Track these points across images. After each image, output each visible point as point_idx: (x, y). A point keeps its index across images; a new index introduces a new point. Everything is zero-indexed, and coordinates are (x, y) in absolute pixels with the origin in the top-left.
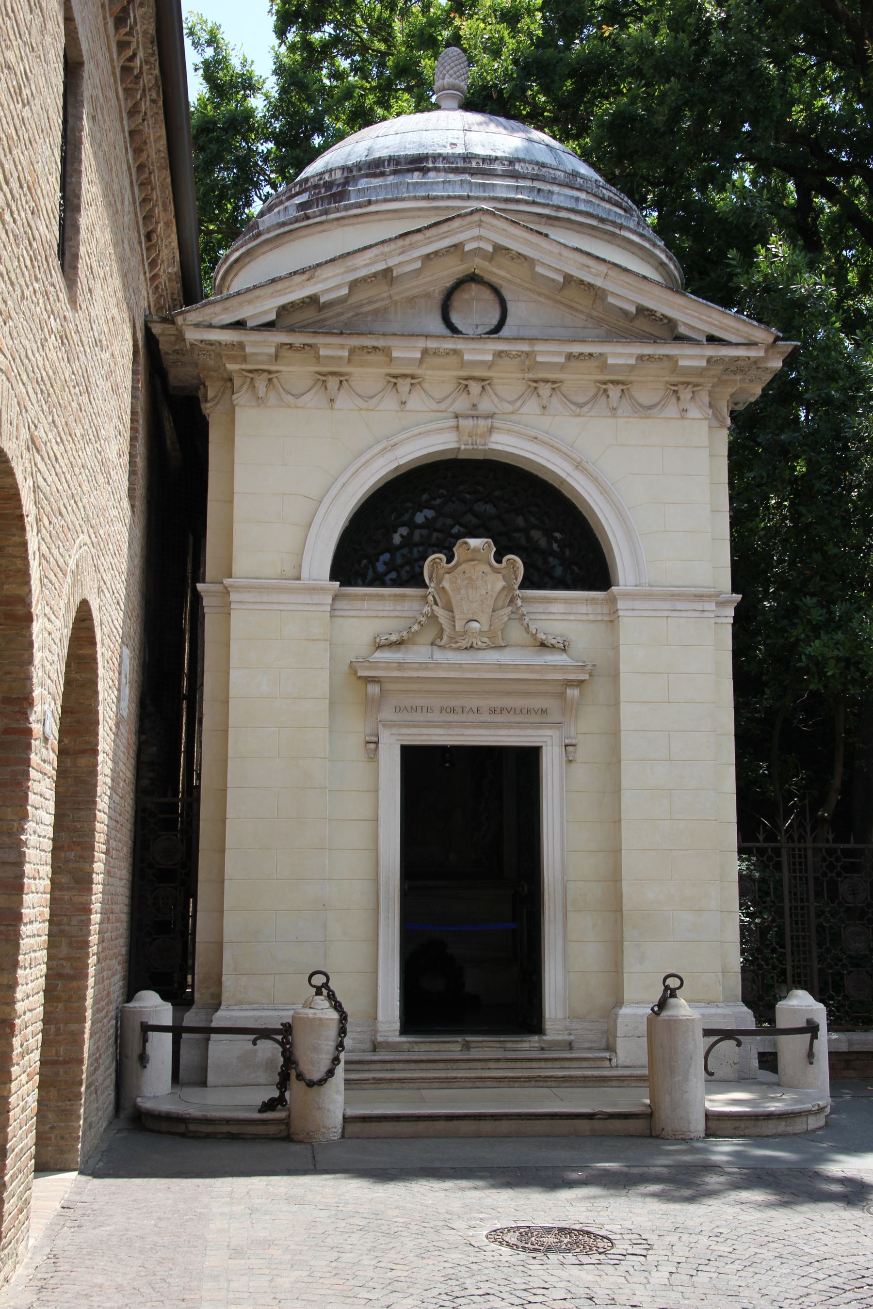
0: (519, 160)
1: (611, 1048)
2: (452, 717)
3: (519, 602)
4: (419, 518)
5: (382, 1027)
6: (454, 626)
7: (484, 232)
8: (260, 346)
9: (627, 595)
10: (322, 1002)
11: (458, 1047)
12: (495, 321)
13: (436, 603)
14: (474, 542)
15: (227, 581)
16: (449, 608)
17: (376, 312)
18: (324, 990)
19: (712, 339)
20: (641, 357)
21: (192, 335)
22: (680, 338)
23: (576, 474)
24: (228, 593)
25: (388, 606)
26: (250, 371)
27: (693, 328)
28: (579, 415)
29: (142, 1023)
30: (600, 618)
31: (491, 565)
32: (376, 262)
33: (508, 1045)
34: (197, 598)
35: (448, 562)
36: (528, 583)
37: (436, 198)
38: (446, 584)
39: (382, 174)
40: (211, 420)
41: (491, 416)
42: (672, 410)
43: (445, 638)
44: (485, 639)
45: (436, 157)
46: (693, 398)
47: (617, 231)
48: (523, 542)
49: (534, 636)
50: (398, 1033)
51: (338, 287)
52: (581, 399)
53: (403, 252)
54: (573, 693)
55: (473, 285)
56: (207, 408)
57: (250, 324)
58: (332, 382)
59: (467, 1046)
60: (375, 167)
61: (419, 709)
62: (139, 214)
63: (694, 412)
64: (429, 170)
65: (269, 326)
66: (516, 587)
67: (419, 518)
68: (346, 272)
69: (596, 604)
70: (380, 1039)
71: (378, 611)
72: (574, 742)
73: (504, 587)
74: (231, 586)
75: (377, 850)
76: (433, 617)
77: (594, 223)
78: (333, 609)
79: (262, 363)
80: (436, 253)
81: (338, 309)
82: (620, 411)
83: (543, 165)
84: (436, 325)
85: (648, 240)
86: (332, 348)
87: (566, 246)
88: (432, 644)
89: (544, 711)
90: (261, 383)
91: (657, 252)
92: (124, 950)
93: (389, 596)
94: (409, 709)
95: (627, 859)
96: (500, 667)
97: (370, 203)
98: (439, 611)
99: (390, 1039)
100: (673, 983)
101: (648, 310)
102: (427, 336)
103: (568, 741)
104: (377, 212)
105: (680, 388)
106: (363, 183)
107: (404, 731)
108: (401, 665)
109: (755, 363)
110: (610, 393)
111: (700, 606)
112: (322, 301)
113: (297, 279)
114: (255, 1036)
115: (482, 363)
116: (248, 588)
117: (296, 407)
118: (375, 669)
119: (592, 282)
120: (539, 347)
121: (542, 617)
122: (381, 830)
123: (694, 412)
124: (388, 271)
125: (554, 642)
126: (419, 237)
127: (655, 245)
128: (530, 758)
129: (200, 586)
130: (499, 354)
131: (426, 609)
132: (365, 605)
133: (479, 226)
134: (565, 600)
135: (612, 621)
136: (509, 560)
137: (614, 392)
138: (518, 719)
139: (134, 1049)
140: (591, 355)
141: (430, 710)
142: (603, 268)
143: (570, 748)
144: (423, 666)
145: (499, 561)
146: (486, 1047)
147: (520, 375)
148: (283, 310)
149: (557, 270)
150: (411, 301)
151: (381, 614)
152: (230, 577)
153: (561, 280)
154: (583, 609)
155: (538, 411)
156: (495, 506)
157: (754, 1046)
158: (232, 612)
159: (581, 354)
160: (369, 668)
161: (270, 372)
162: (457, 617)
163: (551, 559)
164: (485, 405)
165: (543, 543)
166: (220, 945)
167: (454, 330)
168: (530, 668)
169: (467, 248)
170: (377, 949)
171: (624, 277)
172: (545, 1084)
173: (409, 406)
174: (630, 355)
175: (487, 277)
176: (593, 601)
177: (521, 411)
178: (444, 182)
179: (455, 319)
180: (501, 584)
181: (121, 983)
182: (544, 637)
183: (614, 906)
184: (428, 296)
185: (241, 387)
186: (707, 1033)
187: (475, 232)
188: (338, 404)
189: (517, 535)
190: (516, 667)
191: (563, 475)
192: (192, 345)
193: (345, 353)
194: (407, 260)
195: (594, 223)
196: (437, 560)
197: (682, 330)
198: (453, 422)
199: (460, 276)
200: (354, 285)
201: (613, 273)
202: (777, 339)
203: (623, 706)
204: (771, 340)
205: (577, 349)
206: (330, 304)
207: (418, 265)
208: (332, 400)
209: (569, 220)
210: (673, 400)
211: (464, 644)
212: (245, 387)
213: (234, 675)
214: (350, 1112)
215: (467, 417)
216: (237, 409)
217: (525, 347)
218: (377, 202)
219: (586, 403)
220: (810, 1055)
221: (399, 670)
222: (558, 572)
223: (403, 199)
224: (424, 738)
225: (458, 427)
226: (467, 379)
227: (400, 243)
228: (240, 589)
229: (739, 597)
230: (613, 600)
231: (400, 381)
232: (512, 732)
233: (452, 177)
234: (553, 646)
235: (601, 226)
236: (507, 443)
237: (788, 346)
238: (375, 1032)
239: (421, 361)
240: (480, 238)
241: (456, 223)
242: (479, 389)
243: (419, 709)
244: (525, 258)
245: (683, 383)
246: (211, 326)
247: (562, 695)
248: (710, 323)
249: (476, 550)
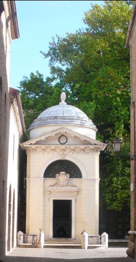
8: (34, 147)
21: (25, 146)
34: (25, 180)
54: (76, 193)
84: (57, 142)
86: (44, 147)
90: (34, 151)
148: (37, 142)
220: (105, 240)
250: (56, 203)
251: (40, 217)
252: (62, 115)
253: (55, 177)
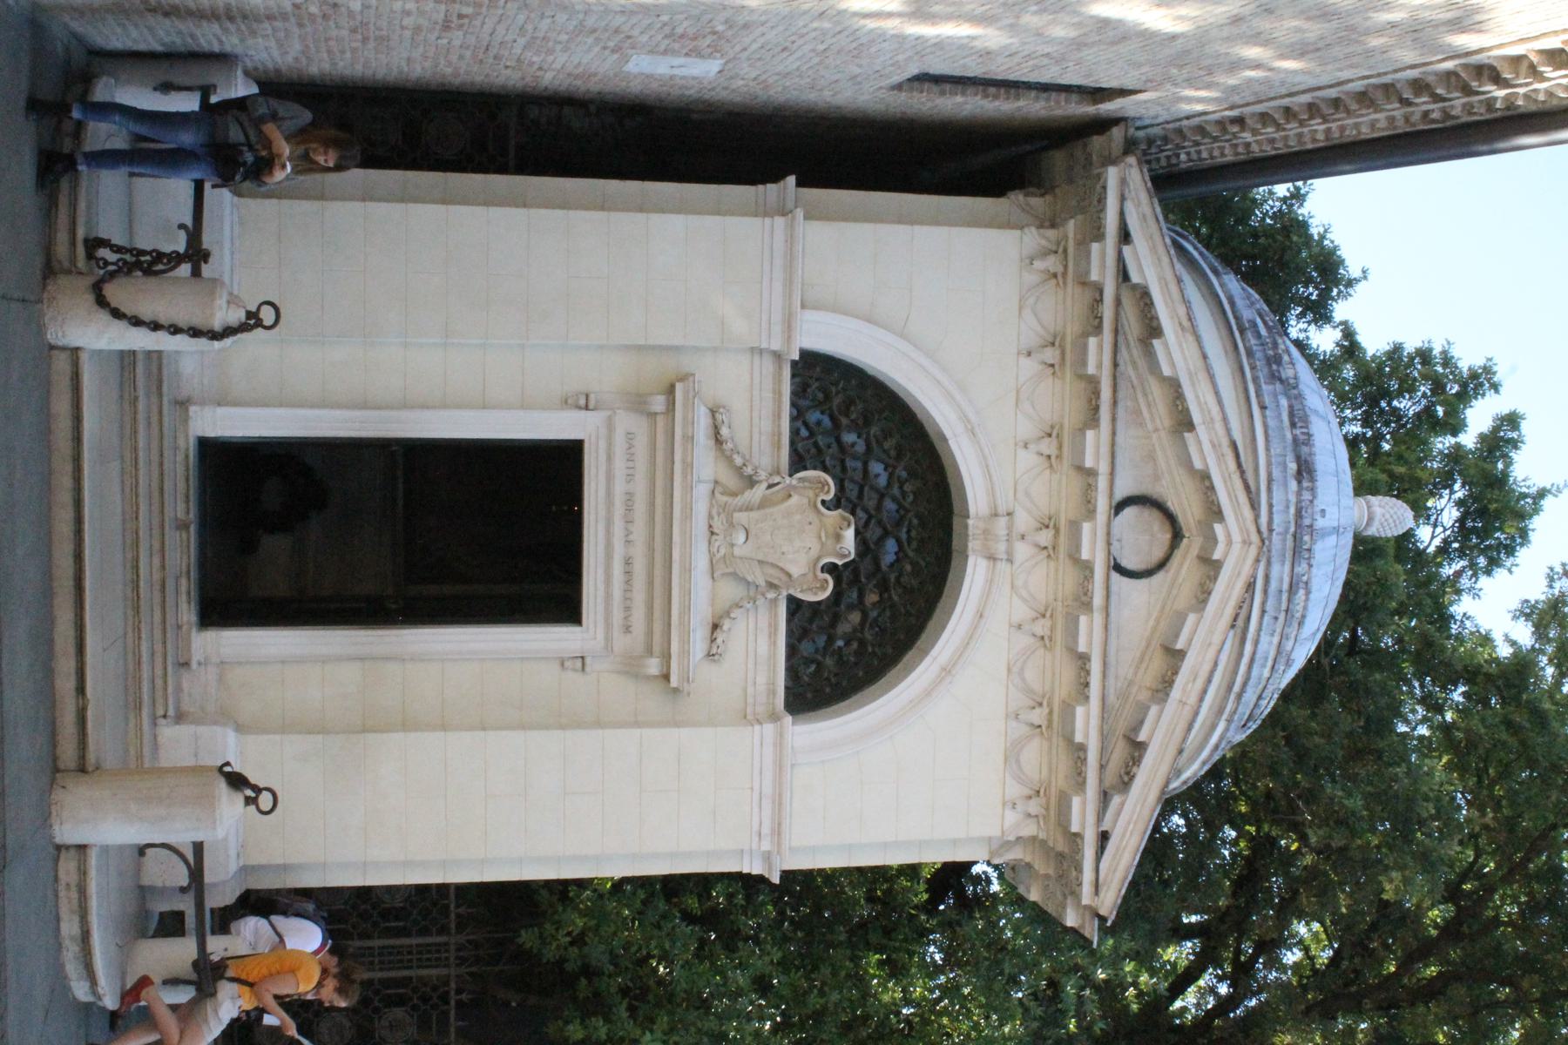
0: (1308, 593)
1: (180, 718)
2: (619, 510)
3: (771, 595)
4: (876, 468)
5: (208, 412)
7: (1237, 547)
9: (781, 735)
10: (236, 316)
11: (181, 515)
12: (1125, 563)
13: (770, 486)
14: (849, 535)
15: (800, 213)
16: (764, 504)
17: (1138, 412)
18: (252, 321)
19: (1104, 837)
20: (1082, 748)
21: (1112, 174)
22: (1105, 797)
23: (935, 668)
24: (784, 215)
25: (766, 425)
26: (1065, 251)
27: (1118, 814)
28: (1009, 670)
29: (215, 87)
30: (750, 700)
31: (818, 559)
32: (1202, 410)
33: (184, 581)
35: (823, 502)
36: (795, 606)
37: (1269, 489)
38: (795, 499)
39: (1293, 425)
40: (1001, 200)
41: (1010, 561)
42: (1015, 790)
43: (725, 498)
44: (723, 551)
45: (1312, 490)
46: (1029, 815)
47: (1225, 716)
48: (845, 601)
49: (727, 614)
50: (201, 434)
51: (1173, 365)
52: (1030, 675)
53: (1214, 446)
54: (653, 666)
55: (1168, 536)
56: (1017, 197)
57: (1126, 250)
58: (1051, 355)
59: (183, 526)
60: (1298, 418)
61: (631, 464)
62: (1272, 104)
63: (1011, 817)
64: (1299, 482)
65: (1123, 275)
66: (792, 592)
67: (876, 468)
68: (1190, 374)
70: (192, 409)
71: (760, 412)
72: (588, 669)
73: (790, 576)
74: (794, 218)
75: (444, 406)
76: (751, 482)
77: (1236, 688)
78: (761, 351)
79: (1076, 265)
80: (1212, 488)
81: (1142, 363)
82: (1014, 724)
83: (1301, 624)
85: (1211, 755)
86: (1097, 354)
87: (1220, 651)
88: (716, 482)
89: (627, 629)
91: (1196, 766)
92: (314, 70)
95: (433, 739)
96: (687, 570)
97: (1263, 408)
98: (759, 491)
99: (191, 424)
100: (265, 800)
101: (1141, 757)
102: (1112, 473)
103: (588, 661)
104: (1251, 416)
105: (1043, 800)
106: (1284, 402)
107: (603, 444)
108: (689, 439)
109: (1073, 893)
110: (1038, 710)
111: (766, 830)
112: (1156, 342)
113: (1182, 311)
114: (189, 223)
115: (1078, 547)
116: (791, 240)
117: (1021, 309)
118: (685, 406)
119: (1176, 686)
120: (1098, 618)
121: (752, 625)
122: (472, 413)
123: (1011, 817)
124: (1190, 426)
125: (719, 641)
126: (1232, 465)
127: (1204, 763)
128: (567, 609)
129: (791, 180)
130: (1087, 567)
131: (763, 475)
132: (768, 395)
133: (1244, 542)
134: (772, 656)
135: (746, 718)
137: (1038, 716)
138: (617, 592)
139: (178, 78)
140: (1087, 685)
141: (630, 477)
142: (1193, 700)
143: (579, 663)
144: (688, 466)
146: (182, 552)
147: (1060, 595)
148: (1144, 295)
149: (1190, 641)
150: (1151, 457)
151: (755, 414)
152: (806, 218)
153: (1179, 646)
154: (762, 680)
155: (1016, 619)
156: (892, 565)
157: (186, 905)
158: (757, 221)
159: (1088, 673)
160: (686, 398)
161: (1065, 274)
163: (824, 638)
164: (1022, 551)
165: (844, 628)
166: (322, 197)
167: (1120, 507)
168: (686, 609)
169: (1218, 528)
170: (312, 406)
171: (1182, 725)
172: (130, 630)
173: (1022, 453)
174: (1087, 735)
175: (1178, 554)
176: (772, 692)
177: (1015, 599)
178: (1288, 501)
179: (1130, 512)
180: (795, 571)
181: (270, 66)
182: (725, 628)
183: (370, 724)
184: (1157, 478)
185: (1044, 237)
186: (198, 848)
187: (1237, 538)
188: (1024, 361)
189: (855, 595)
190: (687, 593)
191: (934, 652)
192: (1099, 176)
193: (1091, 370)
194: (1206, 447)
195: (1236, 688)
197: (1116, 800)
198: (1002, 509)
199: (1181, 519)
200: (1174, 386)
201: (1187, 712)
202: (1102, 919)
203: (637, 732)
204: (1102, 912)
205: (1095, 666)
206: (1150, 354)
207: (1198, 465)
208: (1029, 354)
209: (1240, 655)
210: (1027, 792)
211: (718, 525)
212: (1043, 242)
213: (677, 222)
214: (84, 357)
215: (1010, 527)
216: (1017, 232)
217: (1098, 601)
218: (1264, 417)
219: (1024, 680)
222: (806, 648)
223: (1268, 449)
225: (996, 515)
226: (1057, 530)
227: (1225, 442)
228: (791, 227)
229: (776, 880)
230: (774, 717)
231: (1054, 440)
232: (601, 587)
233: (1292, 510)
234: (713, 640)
235: (1232, 697)
236: (975, 578)
237: (1092, 932)
238: (203, 403)
239: (1080, 468)
240: (1230, 543)
241: (1248, 513)
242: (1044, 544)
244: (1204, 602)
245: (1048, 803)
246: (1123, 199)
247: (649, 651)
248: (1124, 835)
249: (838, 538)
250: (553, 471)
251: (396, 320)
252: (1320, 523)
253: (798, 462)
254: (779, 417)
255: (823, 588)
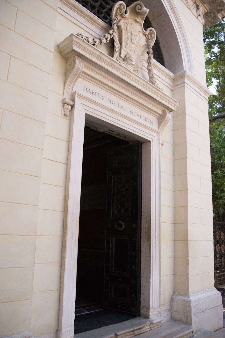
6: (120, 53)
30: (168, 86)
38: (122, 23)
69: (169, 78)
76: (112, 41)
93: (87, 16)
94: (91, 92)
132: (72, 13)
136: (150, 31)
141: (102, 97)
145: (146, 30)
162: (124, 48)
196: (122, 7)
221: (98, 58)
224: (99, 113)
243: (97, 94)
254: (82, 12)
255: (151, 34)
